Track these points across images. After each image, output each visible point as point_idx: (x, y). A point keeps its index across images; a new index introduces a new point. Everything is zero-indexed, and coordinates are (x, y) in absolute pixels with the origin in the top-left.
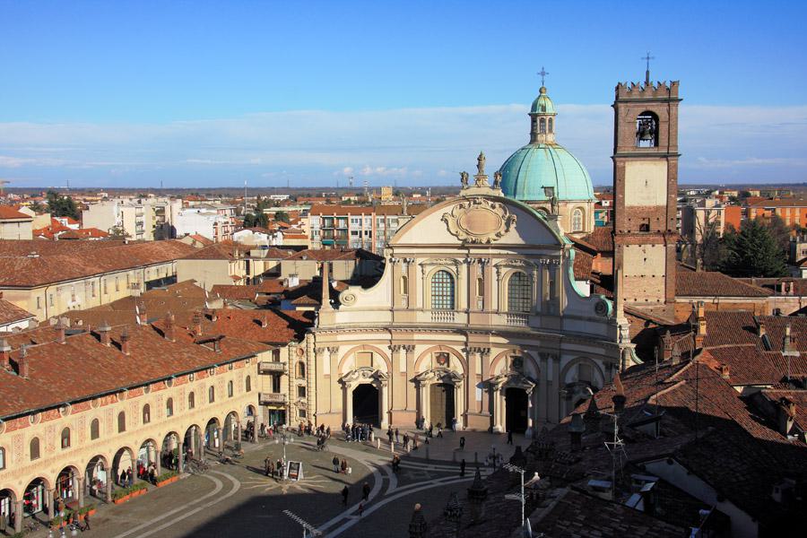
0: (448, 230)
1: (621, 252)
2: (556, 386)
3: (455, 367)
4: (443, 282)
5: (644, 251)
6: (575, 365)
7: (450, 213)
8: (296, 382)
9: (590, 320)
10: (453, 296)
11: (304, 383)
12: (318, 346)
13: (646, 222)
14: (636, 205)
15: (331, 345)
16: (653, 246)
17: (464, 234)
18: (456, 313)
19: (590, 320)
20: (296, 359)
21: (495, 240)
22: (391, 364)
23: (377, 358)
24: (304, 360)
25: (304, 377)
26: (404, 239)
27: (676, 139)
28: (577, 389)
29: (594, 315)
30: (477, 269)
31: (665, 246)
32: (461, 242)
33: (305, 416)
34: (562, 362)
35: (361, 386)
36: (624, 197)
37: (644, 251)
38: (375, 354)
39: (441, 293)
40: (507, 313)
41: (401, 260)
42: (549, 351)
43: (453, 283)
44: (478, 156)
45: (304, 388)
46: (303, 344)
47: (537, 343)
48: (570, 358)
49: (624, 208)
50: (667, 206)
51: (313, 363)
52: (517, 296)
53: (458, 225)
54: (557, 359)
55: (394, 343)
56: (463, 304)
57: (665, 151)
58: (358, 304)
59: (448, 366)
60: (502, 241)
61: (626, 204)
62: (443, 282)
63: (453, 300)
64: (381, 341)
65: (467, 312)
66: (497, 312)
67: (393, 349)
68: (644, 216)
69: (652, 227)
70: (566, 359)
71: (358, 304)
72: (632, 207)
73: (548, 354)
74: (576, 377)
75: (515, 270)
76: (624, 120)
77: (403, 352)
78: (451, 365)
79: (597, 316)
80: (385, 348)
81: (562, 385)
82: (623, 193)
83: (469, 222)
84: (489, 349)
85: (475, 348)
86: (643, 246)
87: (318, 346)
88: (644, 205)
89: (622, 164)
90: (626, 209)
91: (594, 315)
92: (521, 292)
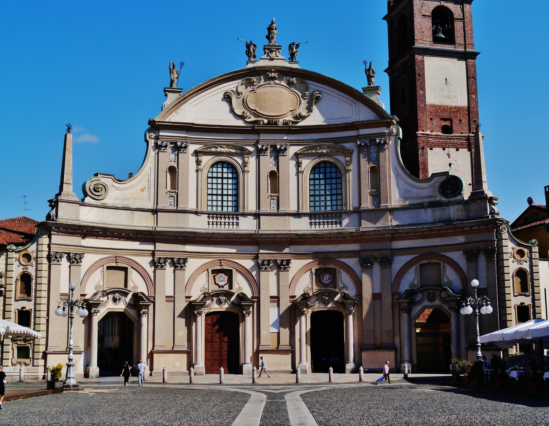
0: (232, 111)
1: (425, 155)
2: (387, 300)
3: (240, 288)
4: (222, 178)
5: (449, 155)
6: (414, 267)
7: (234, 90)
8: (15, 306)
9: (433, 205)
10: (237, 195)
11: (29, 306)
12: (54, 249)
13: (448, 123)
14: (437, 103)
15: (72, 250)
16: (457, 150)
17: (252, 116)
18: (240, 218)
19: (433, 205)
20: (17, 271)
21: (293, 122)
22: (152, 283)
23: (134, 276)
24: (31, 270)
25: (29, 294)
26: (176, 117)
27: (472, 38)
28: (419, 297)
29: (440, 198)
30: (268, 164)
31: (470, 150)
32: (249, 125)
33: (27, 357)
34: (393, 266)
35: (110, 315)
36: (424, 95)
37: (449, 155)
38: (129, 268)
39: (220, 192)
40: (311, 216)
41: (169, 145)
42: (376, 254)
43: (236, 178)
44: (267, 25)
45: (28, 313)
46: (32, 249)
47: (355, 247)
48: (408, 258)
49: (425, 105)
50: (469, 107)
51: (45, 274)
52: (323, 192)
53: (244, 103)
54: (386, 262)
55: (158, 255)
56: (252, 207)
57: (461, 49)
58: (108, 200)
59: (231, 287)
60: (302, 123)
61: (427, 104)
62: (222, 178)
63: (237, 201)
64: (141, 252)
65: (257, 216)
66: (297, 215)
67: (157, 264)
68: (446, 115)
69: (455, 128)
70: (399, 262)
71: (108, 200)
72: (434, 106)
73: (375, 258)
74: (416, 282)
75: (317, 161)
76: (420, 12)
77: (169, 269)
78: (235, 286)
79: (444, 199)
80: (145, 262)
81: (395, 293)
82: (423, 89)
83: (258, 101)
84: (288, 262)
85: (269, 261)
86: (447, 149)
87: (54, 249)
88: (445, 104)
89: (421, 57)
90: (428, 108)
91: (440, 198)
92: (328, 187)
